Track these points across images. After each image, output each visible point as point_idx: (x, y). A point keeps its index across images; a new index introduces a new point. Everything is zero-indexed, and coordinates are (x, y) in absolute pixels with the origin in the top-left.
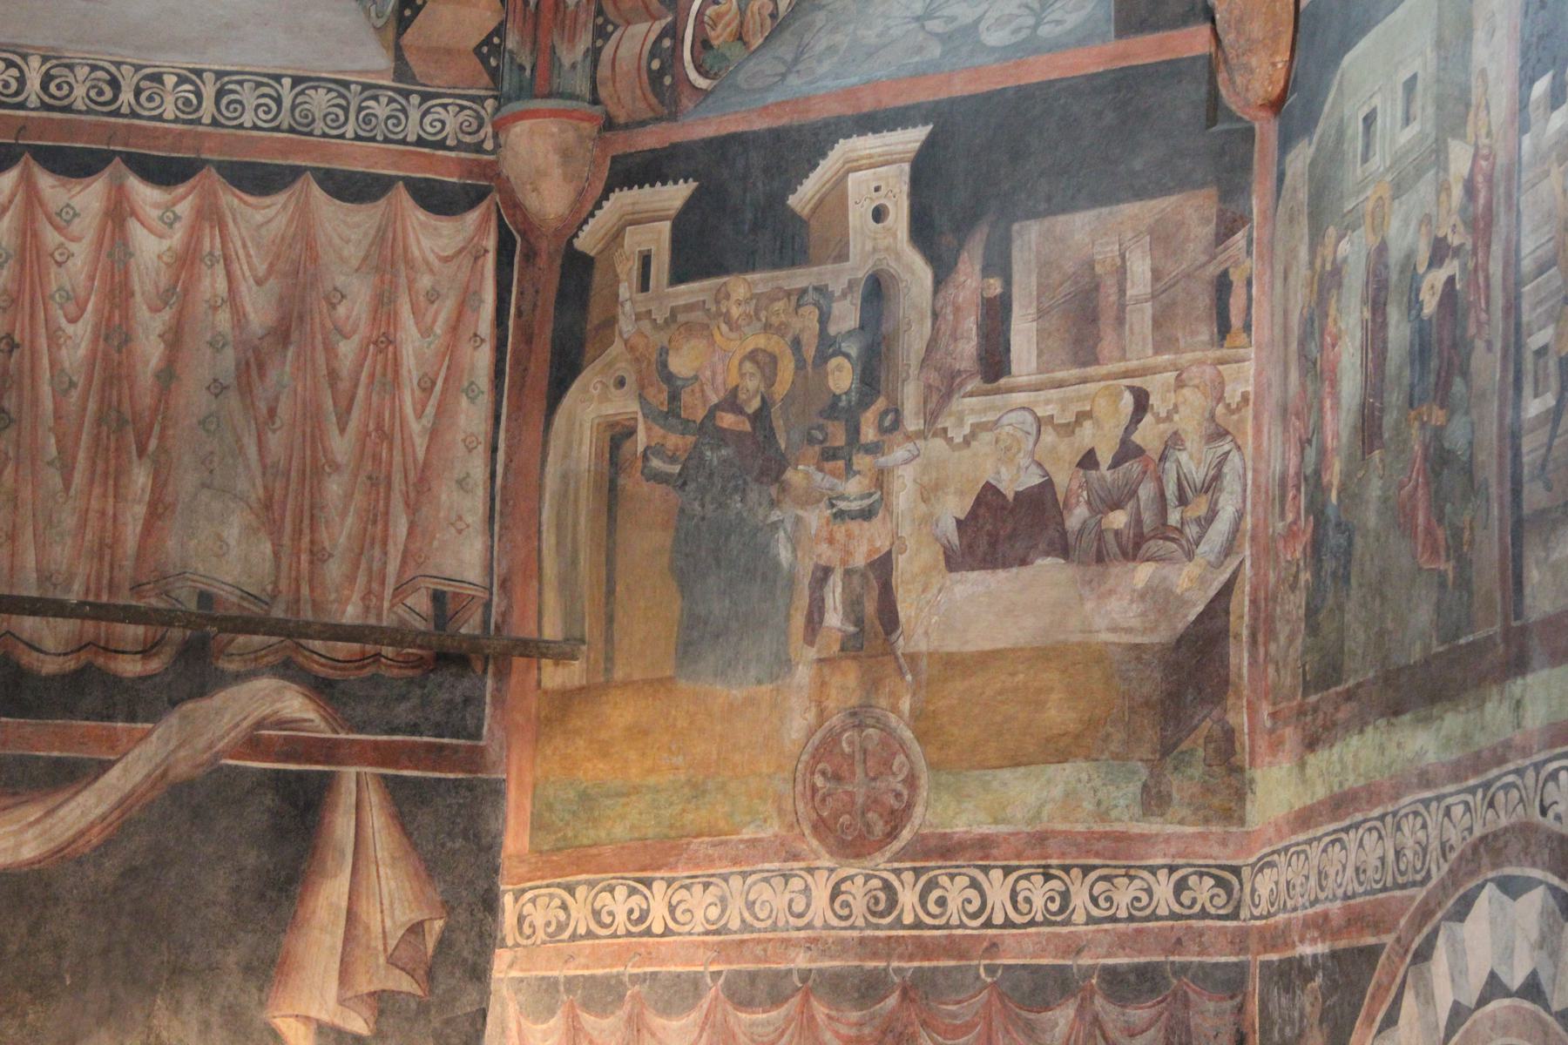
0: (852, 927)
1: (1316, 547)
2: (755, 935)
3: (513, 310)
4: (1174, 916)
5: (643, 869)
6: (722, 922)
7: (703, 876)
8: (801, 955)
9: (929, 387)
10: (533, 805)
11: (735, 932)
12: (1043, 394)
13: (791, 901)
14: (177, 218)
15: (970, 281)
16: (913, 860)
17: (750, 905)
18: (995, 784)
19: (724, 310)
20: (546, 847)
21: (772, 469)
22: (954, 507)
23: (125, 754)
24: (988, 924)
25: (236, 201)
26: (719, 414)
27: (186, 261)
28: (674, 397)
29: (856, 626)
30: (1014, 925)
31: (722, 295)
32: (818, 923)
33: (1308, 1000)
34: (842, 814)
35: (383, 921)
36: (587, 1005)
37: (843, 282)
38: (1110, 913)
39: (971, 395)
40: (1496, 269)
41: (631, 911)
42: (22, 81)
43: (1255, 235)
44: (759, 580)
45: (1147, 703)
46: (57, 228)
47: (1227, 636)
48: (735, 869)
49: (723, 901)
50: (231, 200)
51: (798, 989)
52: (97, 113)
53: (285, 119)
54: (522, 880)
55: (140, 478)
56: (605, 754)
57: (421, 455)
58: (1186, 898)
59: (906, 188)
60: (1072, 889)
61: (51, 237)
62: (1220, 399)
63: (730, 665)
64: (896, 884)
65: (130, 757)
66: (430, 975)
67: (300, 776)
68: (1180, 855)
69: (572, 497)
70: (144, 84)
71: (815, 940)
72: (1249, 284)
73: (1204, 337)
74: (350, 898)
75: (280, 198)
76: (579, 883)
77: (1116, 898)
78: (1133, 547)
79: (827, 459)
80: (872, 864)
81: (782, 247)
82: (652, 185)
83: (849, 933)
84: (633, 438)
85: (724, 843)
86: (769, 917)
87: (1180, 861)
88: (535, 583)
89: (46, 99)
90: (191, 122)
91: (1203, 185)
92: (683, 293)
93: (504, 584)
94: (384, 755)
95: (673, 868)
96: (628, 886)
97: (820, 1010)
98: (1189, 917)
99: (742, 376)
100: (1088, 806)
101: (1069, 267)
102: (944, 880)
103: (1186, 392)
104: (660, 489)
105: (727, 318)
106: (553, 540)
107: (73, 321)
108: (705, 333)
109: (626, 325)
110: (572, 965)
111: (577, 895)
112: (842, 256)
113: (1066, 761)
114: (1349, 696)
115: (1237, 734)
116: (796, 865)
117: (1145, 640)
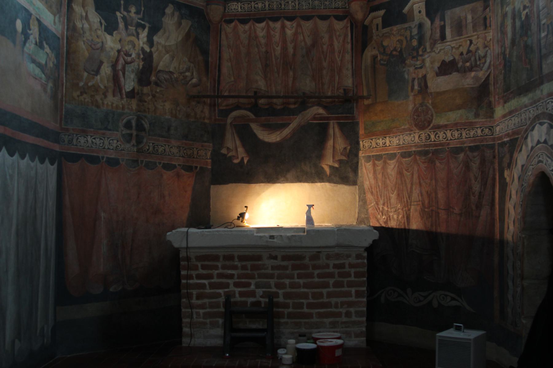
0: (423, 142)
1: (505, 65)
2: (405, 145)
3: (354, 37)
4: (481, 136)
5: (385, 135)
6: (399, 143)
9: (431, 43)
12: (453, 42)
13: (411, 139)
14: (293, 27)
15: (438, 22)
16: (433, 129)
17: (404, 140)
19: (392, 33)
21: (403, 61)
22: (437, 65)
23: (293, 122)
24: (447, 140)
25: (303, 23)
27: (296, 34)
28: (384, 50)
32: (416, 142)
33: (506, 149)
35: (339, 147)
36: (376, 160)
37: (414, 25)
40: (535, 9)
41: (383, 143)
42: (265, 6)
46: (273, 31)
48: (401, 134)
49: (399, 140)
50: (303, 23)
51: (413, 154)
52: (278, 10)
53: (311, 7)
55: (291, 73)
57: (339, 64)
58: (483, 132)
60: (463, 132)
61: (272, 33)
62: (486, 40)
64: (430, 134)
65: (294, 122)
66: (348, 157)
67: (323, 123)
68: (482, 125)
70: (285, 4)
71: (416, 145)
72: (490, 18)
73: (482, 29)
74: (333, 144)
75: (311, 21)
76: (373, 138)
77: (470, 133)
78: (471, 69)
80: (425, 131)
82: (378, 11)
86: (408, 141)
89: (269, 8)
90: (295, 9)
93: (356, 87)
94: (337, 118)
95: (390, 134)
97: (418, 157)
99: (397, 45)
102: (439, 133)
103: (479, 39)
105: (393, 34)
107: (277, 47)
109: (375, 38)
112: (413, 20)
114: (512, 93)
117: (474, 86)
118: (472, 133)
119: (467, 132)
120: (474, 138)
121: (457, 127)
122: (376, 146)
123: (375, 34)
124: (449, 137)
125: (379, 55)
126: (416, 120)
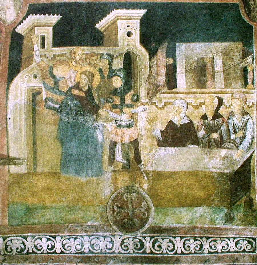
0: (129, 253)
2: (94, 255)
4: (235, 251)
5: (52, 233)
6: (82, 250)
7: (74, 236)
8: (112, 261)
9: (149, 89)
10: (9, 210)
11: (87, 253)
17: (92, 246)
18: (177, 212)
19: (74, 57)
20: (14, 224)
21: (94, 110)
26: (73, 90)
28: (56, 83)
29: (127, 161)
30: (184, 254)
31: (72, 52)
32: (117, 251)
34: (124, 219)
38: (216, 250)
39: (164, 93)
41: (48, 246)
43: (254, 58)
44: (91, 144)
45: (225, 190)
47: (250, 172)
48: (85, 234)
54: (5, 234)
56: (35, 194)
58: (239, 246)
59: (138, 27)
60: (203, 243)
62: (246, 103)
63: (81, 170)
64: (144, 240)
68: (237, 235)
69: (18, 111)
71: (116, 257)
76: (28, 236)
78: (220, 144)
79: (114, 108)
81: (94, 40)
82: (45, 15)
83: (128, 255)
84: (41, 94)
85: (82, 226)
86: (99, 249)
87: (237, 236)
88: (5, 139)
91: (238, 41)
92: (58, 50)
95: (63, 233)
96: (47, 238)
98: (240, 252)
100: (208, 220)
101: (196, 59)
103: (234, 100)
104: (52, 112)
105: (74, 60)
106: (12, 126)
108: (67, 64)
109: (36, 57)
110: (27, 262)
111: (28, 240)
112: (116, 45)
113: (201, 206)
115: (254, 201)
116: (107, 233)
117: (224, 172)
118: (220, 246)
119: (211, 244)
120: (223, 254)
121: (194, 234)
122: (35, 250)
123: (37, 53)
124: (179, 248)
125: (43, 88)
126: (117, 213)
